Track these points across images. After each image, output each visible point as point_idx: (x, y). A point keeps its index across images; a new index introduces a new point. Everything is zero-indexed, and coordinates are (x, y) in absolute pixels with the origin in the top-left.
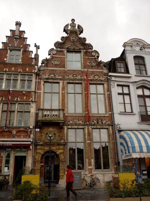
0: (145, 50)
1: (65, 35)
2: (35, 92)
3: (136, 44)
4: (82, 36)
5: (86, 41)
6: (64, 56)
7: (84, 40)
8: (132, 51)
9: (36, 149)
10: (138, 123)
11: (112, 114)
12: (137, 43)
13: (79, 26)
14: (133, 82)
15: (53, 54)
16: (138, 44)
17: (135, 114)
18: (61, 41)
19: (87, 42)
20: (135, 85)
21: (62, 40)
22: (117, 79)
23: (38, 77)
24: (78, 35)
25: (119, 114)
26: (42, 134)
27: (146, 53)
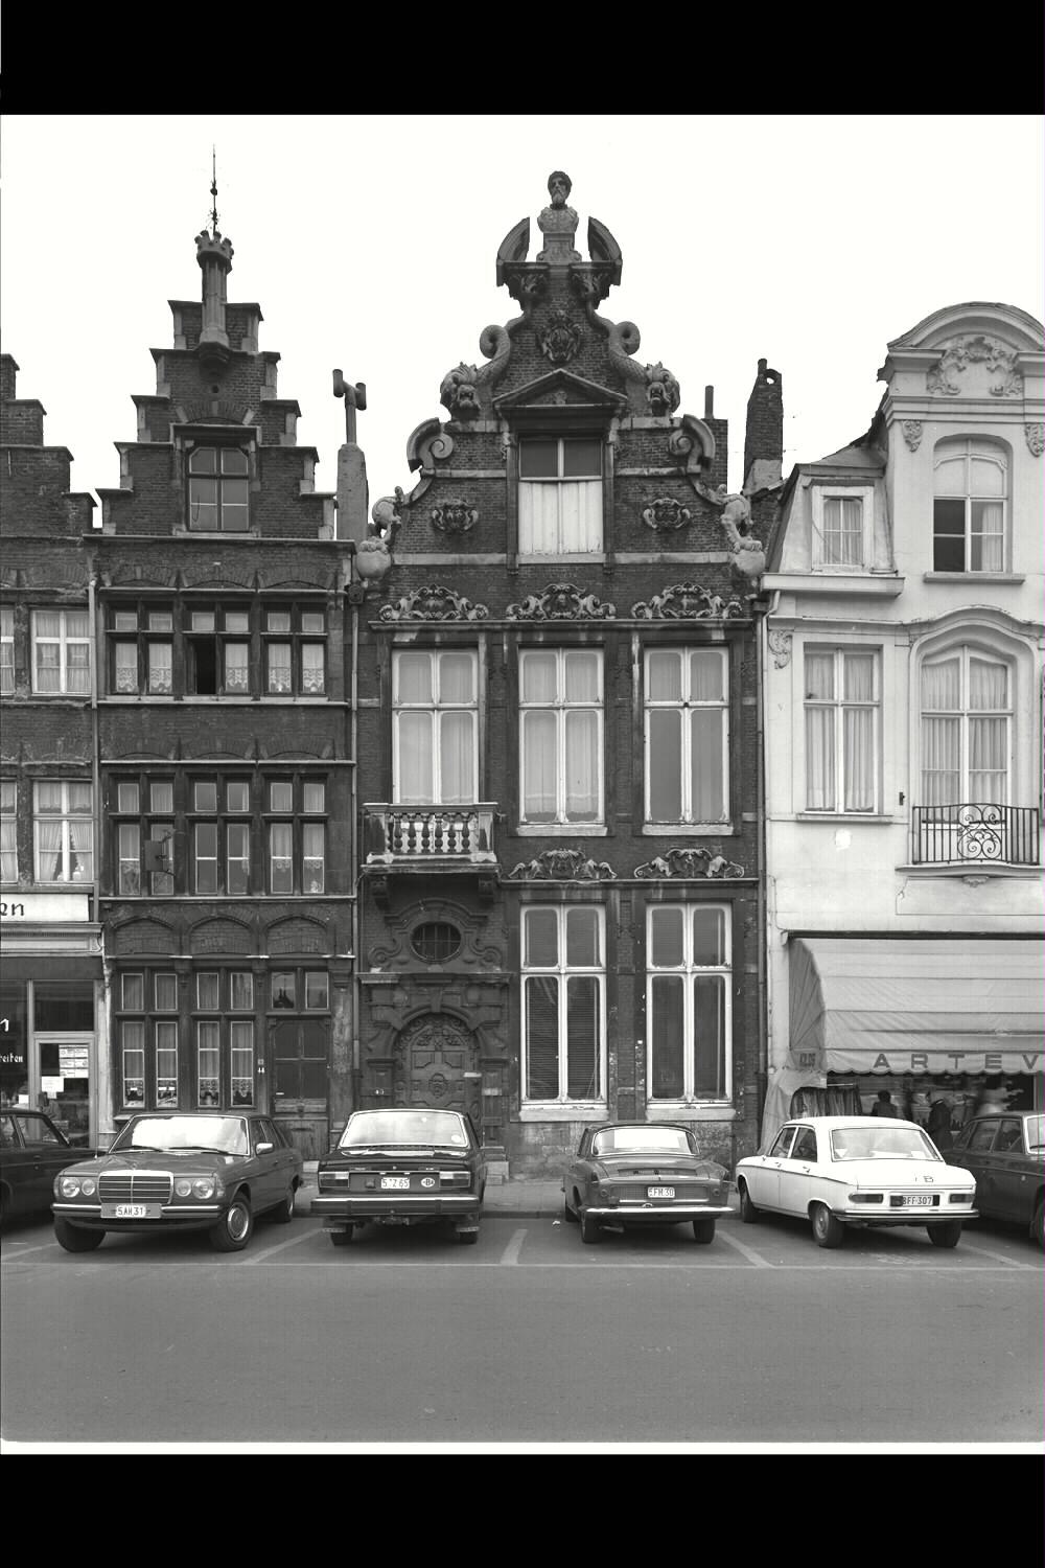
0: (1022, 390)
1: (506, 309)
2: (347, 710)
3: (970, 345)
4: (611, 310)
5: (634, 348)
6: (502, 473)
7: (629, 342)
8: (930, 401)
9: (371, 1007)
10: (898, 870)
11: (756, 823)
12: (971, 338)
13: (599, 237)
14: (904, 628)
15: (438, 462)
16: (979, 342)
17: (889, 824)
18: (481, 361)
19: (643, 357)
20: (916, 645)
21: (488, 351)
22: (812, 613)
23: (356, 617)
24: (590, 306)
25: (798, 822)
27: (1029, 409)
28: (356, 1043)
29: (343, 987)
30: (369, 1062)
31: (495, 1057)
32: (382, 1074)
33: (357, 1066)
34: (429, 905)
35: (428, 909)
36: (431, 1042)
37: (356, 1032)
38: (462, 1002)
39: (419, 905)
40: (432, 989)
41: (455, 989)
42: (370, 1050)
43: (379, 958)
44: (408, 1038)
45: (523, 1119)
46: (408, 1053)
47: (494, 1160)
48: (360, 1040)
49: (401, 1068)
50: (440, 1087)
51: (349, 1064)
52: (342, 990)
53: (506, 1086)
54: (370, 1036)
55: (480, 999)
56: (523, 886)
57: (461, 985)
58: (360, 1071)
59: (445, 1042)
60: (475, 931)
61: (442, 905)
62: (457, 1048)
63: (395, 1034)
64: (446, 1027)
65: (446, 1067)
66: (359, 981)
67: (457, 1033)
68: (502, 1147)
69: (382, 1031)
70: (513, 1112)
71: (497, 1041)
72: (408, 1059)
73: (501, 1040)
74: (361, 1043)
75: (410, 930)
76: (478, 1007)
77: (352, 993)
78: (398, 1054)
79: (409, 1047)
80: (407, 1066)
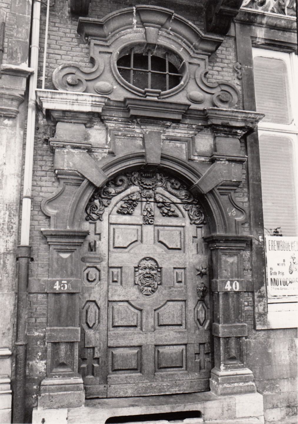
26: (95, 52)
28: (27, 204)
29: (9, 118)
30: (44, 236)
31: (232, 234)
32: (65, 256)
33: (25, 241)
34: (146, 17)
35: (143, 23)
36: (137, 211)
37: (27, 190)
38: (189, 153)
39: (130, 13)
40: (149, 129)
41: (181, 132)
42: (48, 217)
43: (69, 79)
44: (105, 201)
45: (274, 325)
46: (103, 226)
47: (240, 393)
48: (32, 198)
49: (92, 248)
50: (151, 277)
51: (12, 239)
52: (6, 121)
53: (248, 276)
54: (50, 196)
55: (215, 148)
56: (259, 19)
57: (190, 127)
58: (30, 248)
59: (157, 212)
60: (202, 63)
61: (162, 19)
62: (174, 221)
63: (90, 193)
64: (160, 190)
65: (160, 249)
66: (38, 108)
67: (179, 201)
68: (247, 371)
69: (68, 188)
70: (260, 315)
71: (234, 211)
72: (105, 235)
73: (241, 210)
74: (34, 204)
75: (116, 50)
76: (213, 161)
77: (24, 127)
78: (87, 226)
79: (105, 217)
80: (103, 246)
